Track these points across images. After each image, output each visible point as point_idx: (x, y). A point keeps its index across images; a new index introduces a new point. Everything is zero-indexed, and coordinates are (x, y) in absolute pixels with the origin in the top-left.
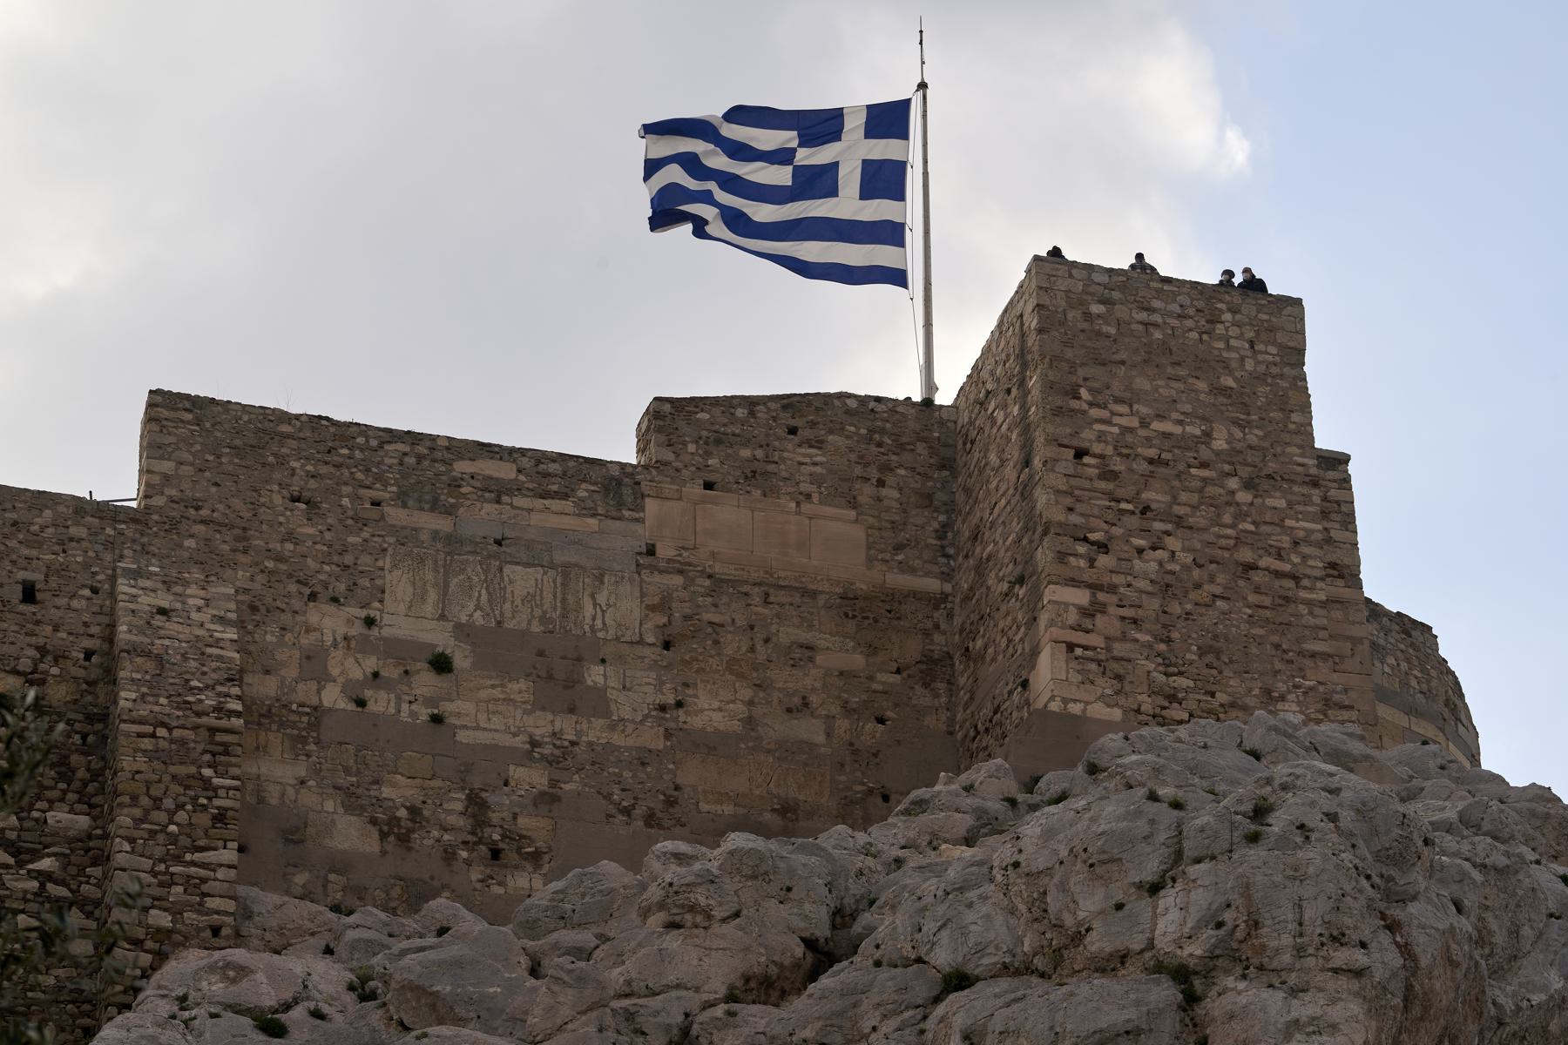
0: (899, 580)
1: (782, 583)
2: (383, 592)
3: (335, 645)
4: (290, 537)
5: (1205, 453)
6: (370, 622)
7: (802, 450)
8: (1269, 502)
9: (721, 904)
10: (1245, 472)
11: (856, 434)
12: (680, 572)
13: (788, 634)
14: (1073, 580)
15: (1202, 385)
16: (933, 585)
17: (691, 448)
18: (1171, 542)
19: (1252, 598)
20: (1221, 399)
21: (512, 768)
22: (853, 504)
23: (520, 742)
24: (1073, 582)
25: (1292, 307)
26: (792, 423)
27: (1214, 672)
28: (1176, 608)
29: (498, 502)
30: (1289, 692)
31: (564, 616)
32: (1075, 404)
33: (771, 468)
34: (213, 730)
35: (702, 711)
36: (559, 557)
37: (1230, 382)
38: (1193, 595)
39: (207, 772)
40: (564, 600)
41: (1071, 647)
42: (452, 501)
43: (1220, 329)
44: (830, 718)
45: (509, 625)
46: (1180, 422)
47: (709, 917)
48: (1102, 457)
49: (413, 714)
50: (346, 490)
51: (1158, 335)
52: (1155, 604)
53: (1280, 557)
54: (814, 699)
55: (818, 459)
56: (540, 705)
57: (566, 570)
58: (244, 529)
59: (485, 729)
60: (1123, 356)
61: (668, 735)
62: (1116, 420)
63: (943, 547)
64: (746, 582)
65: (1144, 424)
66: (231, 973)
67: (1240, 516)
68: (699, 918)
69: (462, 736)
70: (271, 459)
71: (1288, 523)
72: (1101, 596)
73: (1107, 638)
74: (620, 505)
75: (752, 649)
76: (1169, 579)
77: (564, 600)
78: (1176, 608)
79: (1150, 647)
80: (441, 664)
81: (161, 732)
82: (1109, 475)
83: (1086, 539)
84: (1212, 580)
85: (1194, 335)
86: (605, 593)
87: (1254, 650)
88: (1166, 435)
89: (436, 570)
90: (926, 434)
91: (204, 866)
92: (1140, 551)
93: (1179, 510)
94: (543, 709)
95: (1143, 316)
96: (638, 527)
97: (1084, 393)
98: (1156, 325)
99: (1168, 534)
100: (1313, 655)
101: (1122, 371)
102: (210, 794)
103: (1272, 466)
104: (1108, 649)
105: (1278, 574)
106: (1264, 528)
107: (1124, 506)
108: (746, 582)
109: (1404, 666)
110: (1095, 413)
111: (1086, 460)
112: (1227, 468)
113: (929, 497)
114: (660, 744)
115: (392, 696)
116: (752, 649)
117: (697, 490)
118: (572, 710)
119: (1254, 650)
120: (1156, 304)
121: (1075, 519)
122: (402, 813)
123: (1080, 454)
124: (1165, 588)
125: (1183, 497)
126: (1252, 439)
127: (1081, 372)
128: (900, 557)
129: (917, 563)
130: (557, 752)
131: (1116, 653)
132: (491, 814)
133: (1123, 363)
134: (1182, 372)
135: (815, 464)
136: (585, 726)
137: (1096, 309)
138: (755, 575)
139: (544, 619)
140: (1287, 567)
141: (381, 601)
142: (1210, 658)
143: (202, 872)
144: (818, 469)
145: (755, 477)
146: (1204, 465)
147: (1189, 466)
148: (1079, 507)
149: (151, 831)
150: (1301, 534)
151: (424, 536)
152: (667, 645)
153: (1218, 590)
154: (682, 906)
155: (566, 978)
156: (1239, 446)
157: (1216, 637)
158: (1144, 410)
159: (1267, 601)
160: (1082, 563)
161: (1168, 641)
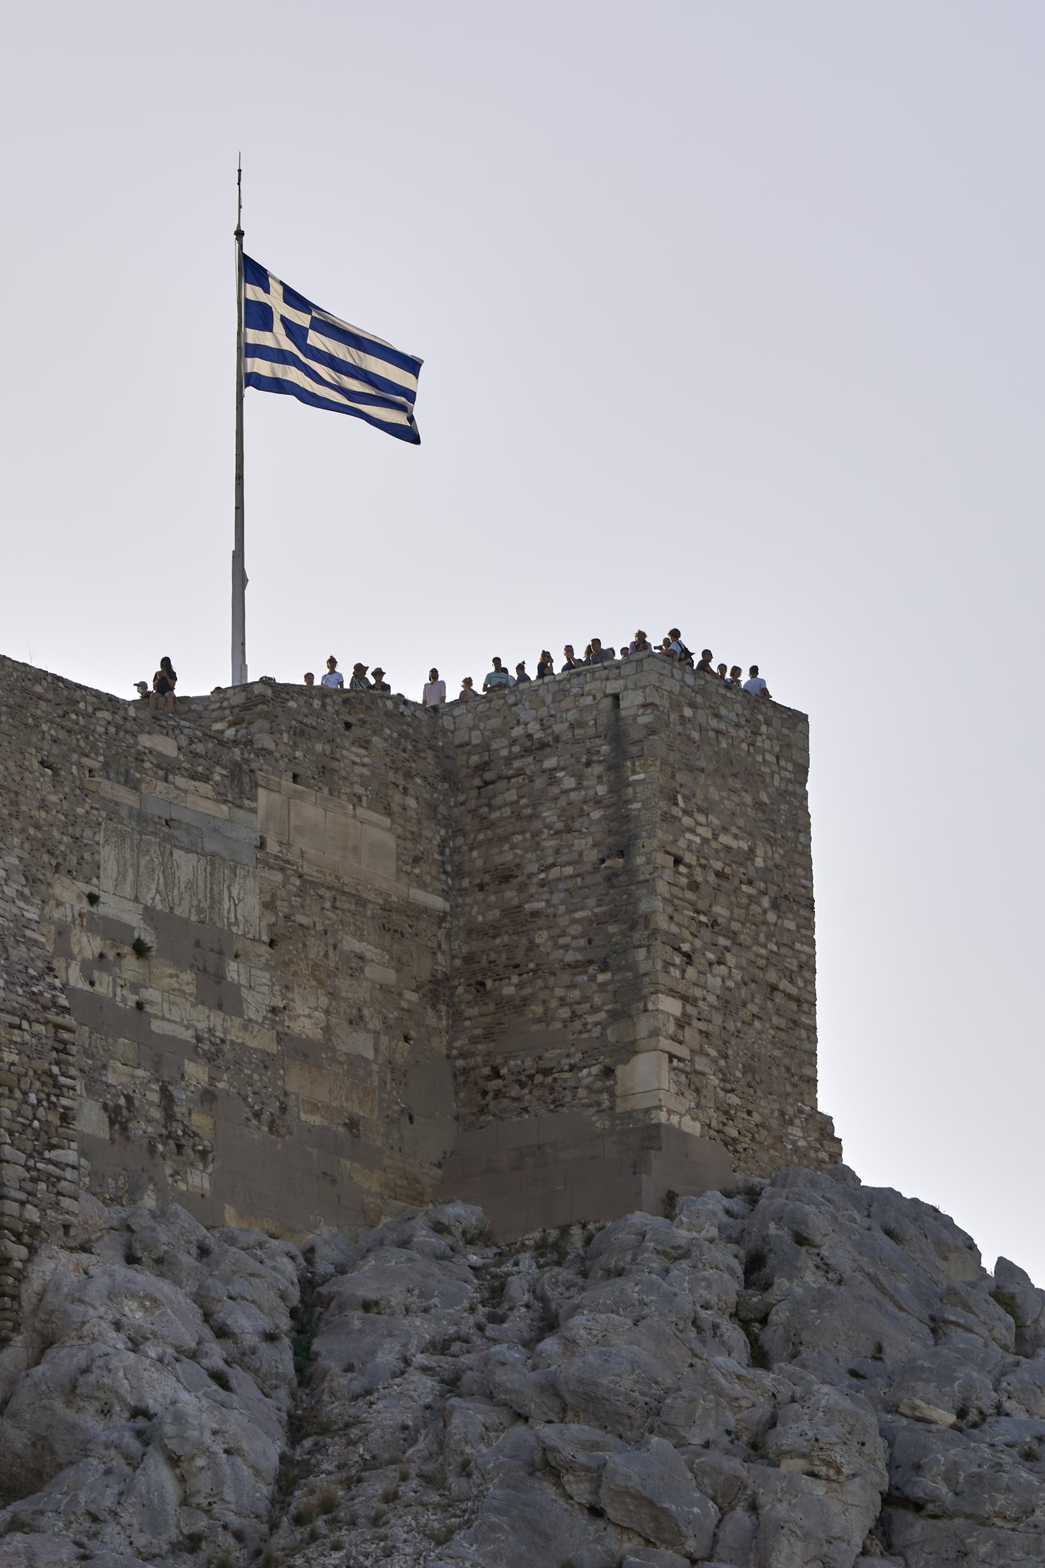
1: (347, 889)
2: (99, 868)
3: (74, 921)
4: (43, 805)
6: (93, 899)
7: (354, 749)
9: (849, 1463)
11: (390, 736)
12: (282, 869)
13: (352, 944)
14: (672, 990)
15: (748, 799)
16: (438, 903)
18: (730, 959)
19: (776, 1020)
21: (186, 1062)
22: (388, 811)
24: (672, 993)
25: (798, 720)
26: (350, 719)
27: (752, 1091)
29: (166, 780)
30: (796, 1116)
31: (212, 907)
34: (58, 1027)
35: (299, 1016)
39: (55, 1070)
40: (212, 889)
41: (671, 1057)
42: (138, 775)
44: (376, 1033)
45: (178, 911)
46: (736, 837)
47: (839, 1472)
49: (124, 999)
50: (75, 757)
54: (366, 1012)
55: (366, 760)
56: (200, 1000)
57: (212, 858)
58: (17, 793)
59: (169, 1020)
60: (702, 764)
61: (279, 1040)
62: (700, 830)
63: (443, 863)
64: (323, 885)
66: (148, 1303)
68: (832, 1472)
69: (156, 1026)
70: (30, 720)
71: (798, 946)
73: (691, 1051)
75: (326, 955)
77: (212, 889)
78: (731, 1026)
80: (140, 949)
81: (25, 1025)
85: (744, 746)
86: (237, 886)
88: (728, 849)
89: (132, 850)
90: (433, 742)
91: (56, 1164)
94: (203, 1003)
95: (714, 723)
96: (251, 817)
101: (702, 779)
102: (58, 1092)
108: (323, 885)
110: (687, 821)
113: (434, 808)
114: (274, 1048)
115: (111, 978)
116: (326, 955)
117: (287, 783)
118: (220, 1007)
120: (723, 711)
122: (122, 1101)
123: (678, 861)
128: (417, 871)
129: (428, 879)
130: (213, 1049)
132: (176, 1109)
133: (702, 770)
135: (364, 765)
136: (229, 1024)
137: (688, 712)
138: (330, 879)
139: (200, 910)
140: (794, 991)
141: (98, 877)
143: (58, 1172)
144: (366, 771)
147: (741, 882)
149: (23, 1124)
151: (124, 812)
152: (272, 944)
153: (755, 1009)
154: (823, 1460)
155: (799, 1533)
161: (726, 1057)
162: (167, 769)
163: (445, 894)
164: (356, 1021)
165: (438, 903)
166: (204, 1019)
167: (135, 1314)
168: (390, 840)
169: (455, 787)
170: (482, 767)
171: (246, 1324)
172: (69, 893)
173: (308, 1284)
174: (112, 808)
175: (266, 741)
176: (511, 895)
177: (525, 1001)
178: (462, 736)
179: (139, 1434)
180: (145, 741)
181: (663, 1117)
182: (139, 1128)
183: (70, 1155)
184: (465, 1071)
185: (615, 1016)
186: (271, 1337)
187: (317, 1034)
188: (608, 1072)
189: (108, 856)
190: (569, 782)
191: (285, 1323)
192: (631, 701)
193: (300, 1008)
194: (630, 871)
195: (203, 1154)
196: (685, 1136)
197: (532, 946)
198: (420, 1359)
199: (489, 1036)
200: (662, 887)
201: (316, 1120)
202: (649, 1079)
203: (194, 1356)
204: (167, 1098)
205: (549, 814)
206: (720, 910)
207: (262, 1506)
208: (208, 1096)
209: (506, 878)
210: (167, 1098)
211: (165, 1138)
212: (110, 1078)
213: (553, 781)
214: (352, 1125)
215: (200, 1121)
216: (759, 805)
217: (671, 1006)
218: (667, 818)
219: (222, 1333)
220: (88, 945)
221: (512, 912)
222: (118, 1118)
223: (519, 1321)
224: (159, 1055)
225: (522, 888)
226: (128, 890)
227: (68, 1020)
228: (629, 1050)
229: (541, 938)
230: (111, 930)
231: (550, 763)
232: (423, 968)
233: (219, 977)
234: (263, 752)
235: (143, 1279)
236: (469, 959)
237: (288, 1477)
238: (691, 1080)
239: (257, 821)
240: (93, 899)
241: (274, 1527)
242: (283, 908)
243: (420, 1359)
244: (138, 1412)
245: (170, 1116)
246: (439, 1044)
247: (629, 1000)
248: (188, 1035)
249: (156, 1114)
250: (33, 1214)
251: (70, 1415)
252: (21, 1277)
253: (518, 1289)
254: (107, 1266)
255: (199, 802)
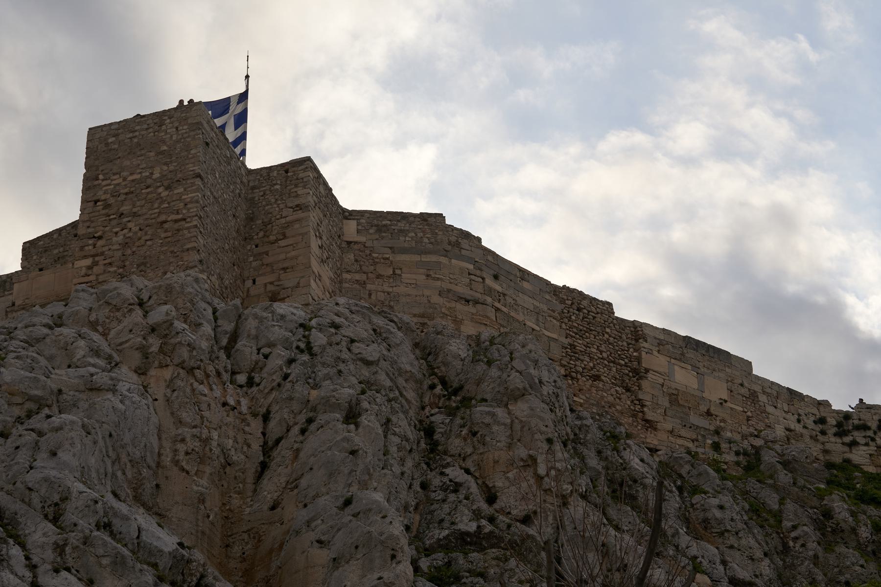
5: (149, 181)
8: (176, 192)
10: (166, 183)
12: (23, 309)
17: (35, 257)
20: (161, 156)
24: (85, 257)
28: (129, 252)
32: (96, 183)
33: (66, 253)
37: (165, 148)
38: (137, 244)
43: (164, 127)
46: (140, 173)
48: (105, 200)
51: (136, 140)
52: (120, 253)
53: (178, 213)
62: (114, 182)
65: (125, 179)
67: (162, 202)
72: (97, 259)
74: (5, 290)
76: (127, 240)
79: (115, 272)
82: (107, 206)
83: (94, 237)
84: (146, 234)
87: (162, 257)
88: (133, 181)
92: (116, 233)
93: (135, 210)
95: (131, 135)
97: (101, 177)
98: (135, 137)
99: (129, 221)
100: (188, 250)
103: (179, 176)
104: (97, 280)
105: (176, 221)
106: (172, 204)
107: (112, 217)
109: (420, 235)
110: (104, 183)
111: (98, 204)
112: (158, 184)
119: (162, 257)
120: (137, 128)
121: (90, 230)
124: (125, 245)
125: (138, 203)
126: (171, 168)
127: (101, 168)
131: (100, 280)
134: (143, 152)
140: (180, 216)
142: (142, 267)
145: (60, 260)
146: (147, 187)
148: (92, 225)
150: (189, 200)
153: (148, 237)
156: (165, 173)
157: (145, 258)
158: (125, 174)
159: (169, 234)
160: (90, 247)
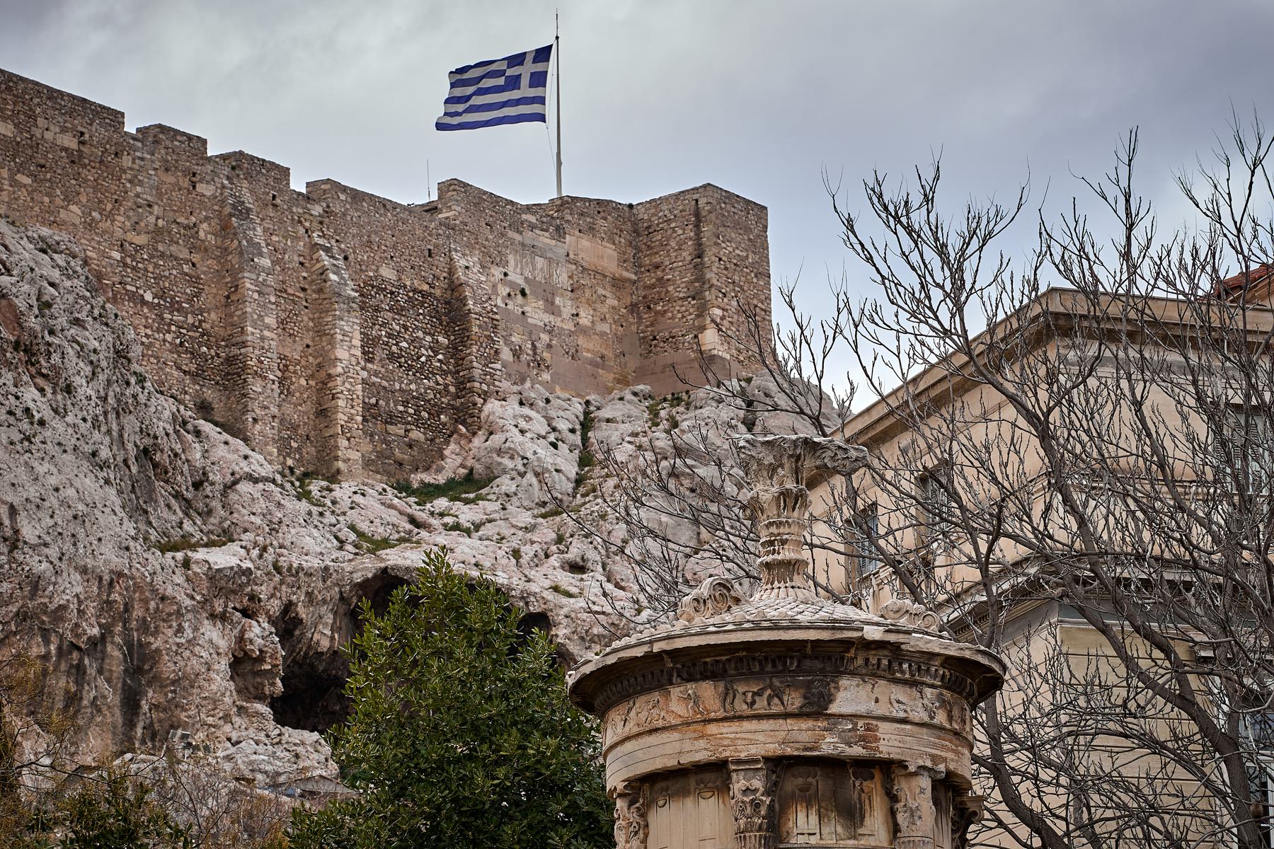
0: (626, 274)
4: (487, 240)
6: (506, 274)
13: (601, 291)
16: (633, 277)
23: (542, 324)
24: (719, 307)
36: (549, 255)
56: (546, 311)
69: (530, 320)
162: (532, 227)
163: (635, 274)
164: (603, 319)
165: (633, 277)
166: (547, 318)
167: (523, 424)
168: (615, 254)
169: (639, 235)
170: (649, 227)
171: (563, 426)
172: (497, 272)
173: (586, 414)
174: (512, 241)
175: (569, 218)
176: (659, 273)
177: (665, 312)
178: (640, 216)
179: (524, 465)
180: (524, 217)
181: (715, 352)
182: (524, 357)
183: (498, 366)
184: (644, 338)
185: (698, 316)
186: (573, 431)
187: (589, 324)
188: (696, 337)
189: (511, 258)
190: (680, 232)
191: (578, 427)
192: (702, 202)
193: (582, 314)
194: (702, 264)
195: (548, 367)
196: (724, 359)
197: (667, 292)
198: (628, 439)
199: (652, 325)
200: (714, 269)
201: (589, 355)
202: (710, 339)
203: (544, 438)
204: (534, 347)
205: (673, 244)
206: (736, 278)
207: (570, 491)
208: (549, 346)
209: (657, 267)
210: (534, 347)
211: (533, 361)
212: (513, 339)
213: (674, 232)
214: (602, 357)
215: (546, 355)
216: (750, 240)
217: (718, 312)
218: (716, 244)
219: (554, 429)
220: (503, 291)
221: (660, 280)
222: (517, 353)
223: (665, 425)
224: (531, 332)
225: (663, 270)
226: (518, 271)
227: (497, 317)
228: (703, 328)
229: (670, 288)
230: (512, 285)
231: (673, 225)
232: (628, 300)
233: (553, 303)
234: (568, 221)
235: (526, 411)
236: (644, 297)
237: (579, 481)
238: (726, 338)
239: (566, 246)
240: (506, 274)
241: (574, 497)
242: (576, 278)
243: (628, 439)
244: (523, 458)
245: (535, 354)
246: (634, 328)
247: (702, 311)
248: (542, 324)
249: (530, 352)
250: (485, 387)
251: (499, 459)
252: (480, 411)
253: (663, 413)
254: (512, 407)
255: (545, 239)
